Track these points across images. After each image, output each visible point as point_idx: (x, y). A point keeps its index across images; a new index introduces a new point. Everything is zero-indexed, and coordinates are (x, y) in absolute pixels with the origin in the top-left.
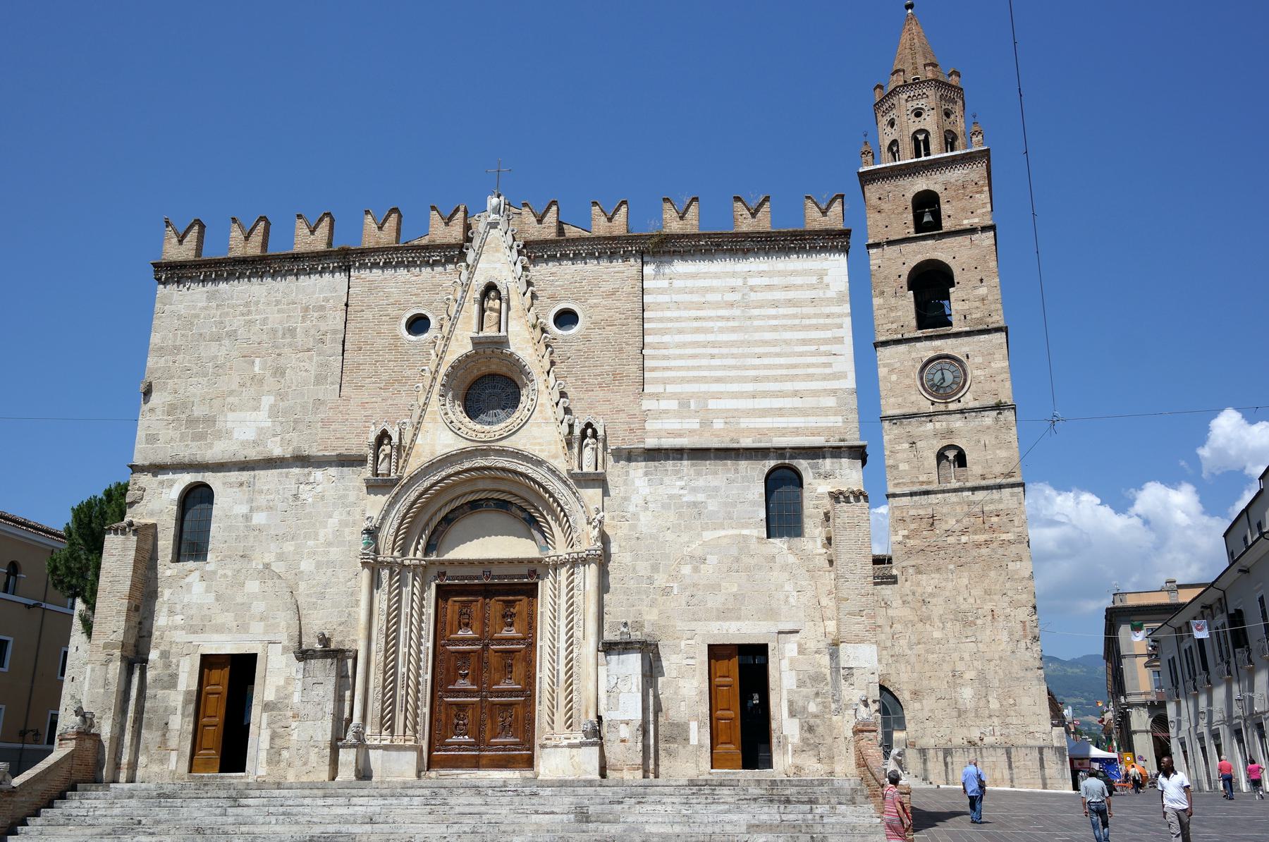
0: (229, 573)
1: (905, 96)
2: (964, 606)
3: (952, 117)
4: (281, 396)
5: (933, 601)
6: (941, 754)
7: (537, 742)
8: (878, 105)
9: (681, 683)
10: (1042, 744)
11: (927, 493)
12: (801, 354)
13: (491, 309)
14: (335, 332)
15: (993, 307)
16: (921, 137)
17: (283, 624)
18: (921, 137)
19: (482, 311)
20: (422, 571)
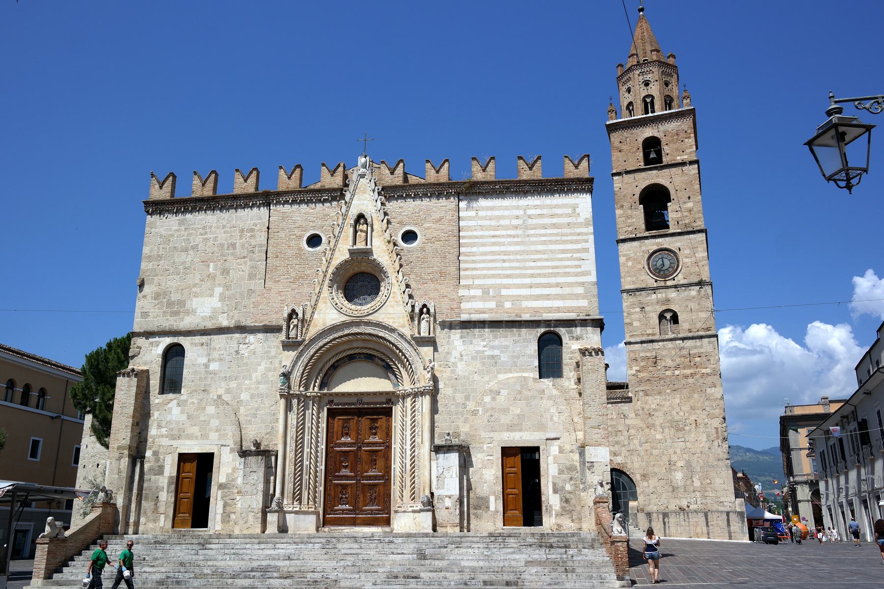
0: (196, 401)
1: (638, 72)
2: (677, 418)
3: (670, 86)
4: (227, 287)
5: (656, 414)
6: (661, 517)
7: (393, 509)
8: (619, 78)
9: (484, 471)
10: (727, 509)
11: (652, 341)
12: (561, 260)
13: (361, 231)
14: (261, 246)
15: (697, 216)
17: (230, 434)
18: (648, 100)
19: (356, 232)
20: (319, 400)
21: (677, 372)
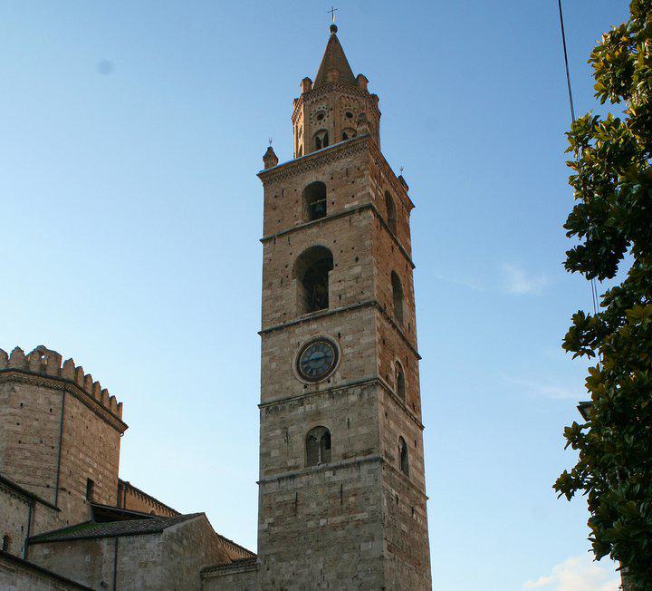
11: (292, 477)
16: (321, 137)
21: (322, 522)
